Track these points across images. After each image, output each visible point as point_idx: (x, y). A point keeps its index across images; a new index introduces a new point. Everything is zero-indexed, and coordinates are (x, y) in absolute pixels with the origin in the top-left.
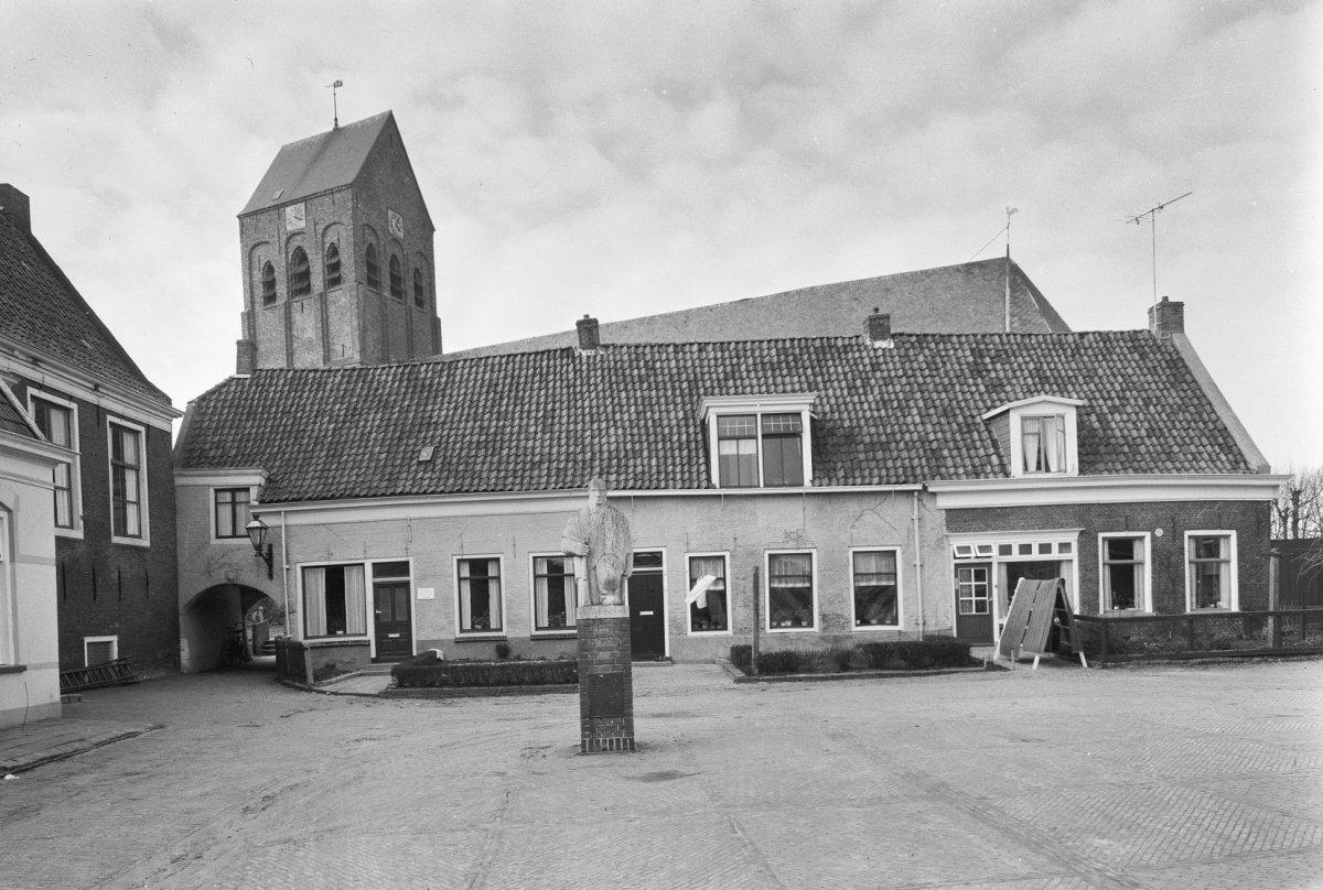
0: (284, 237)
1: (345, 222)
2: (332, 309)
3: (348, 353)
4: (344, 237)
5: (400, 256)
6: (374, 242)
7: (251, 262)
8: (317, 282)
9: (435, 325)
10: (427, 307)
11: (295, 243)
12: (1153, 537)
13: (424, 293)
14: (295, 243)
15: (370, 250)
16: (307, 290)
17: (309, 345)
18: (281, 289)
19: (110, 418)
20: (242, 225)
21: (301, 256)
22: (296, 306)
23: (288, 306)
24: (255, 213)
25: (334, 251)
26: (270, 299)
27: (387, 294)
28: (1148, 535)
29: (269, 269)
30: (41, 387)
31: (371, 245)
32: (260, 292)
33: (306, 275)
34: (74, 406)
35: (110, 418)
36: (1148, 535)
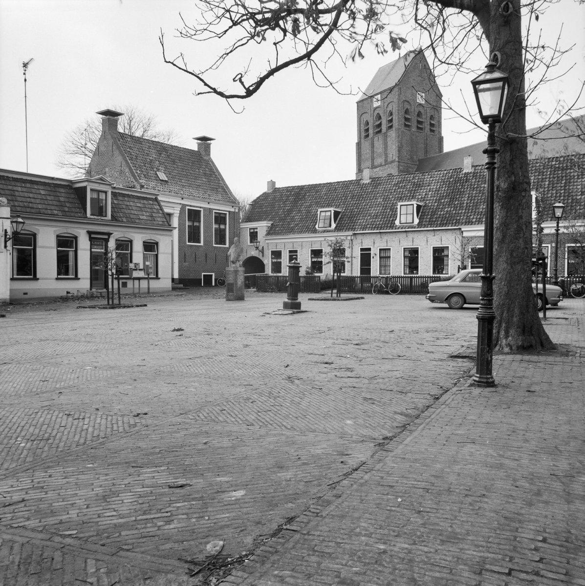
0: (372, 110)
1: (394, 101)
2: (389, 139)
3: (394, 157)
4: (394, 107)
5: (422, 111)
6: (409, 107)
7: (360, 121)
8: (384, 128)
9: (441, 139)
10: (436, 133)
11: (376, 112)
12: (551, 246)
13: (435, 126)
14: (376, 112)
15: (407, 112)
16: (380, 131)
17: (380, 157)
18: (371, 131)
19: (214, 211)
20: (358, 106)
21: (379, 117)
22: (376, 139)
23: (373, 139)
24: (363, 100)
25: (391, 114)
26: (367, 136)
27: (414, 129)
28: (549, 245)
29: (367, 123)
30: (191, 206)
31: (407, 109)
32: (363, 134)
33: (380, 125)
34: (202, 209)
35: (214, 211)
36: (549, 245)
